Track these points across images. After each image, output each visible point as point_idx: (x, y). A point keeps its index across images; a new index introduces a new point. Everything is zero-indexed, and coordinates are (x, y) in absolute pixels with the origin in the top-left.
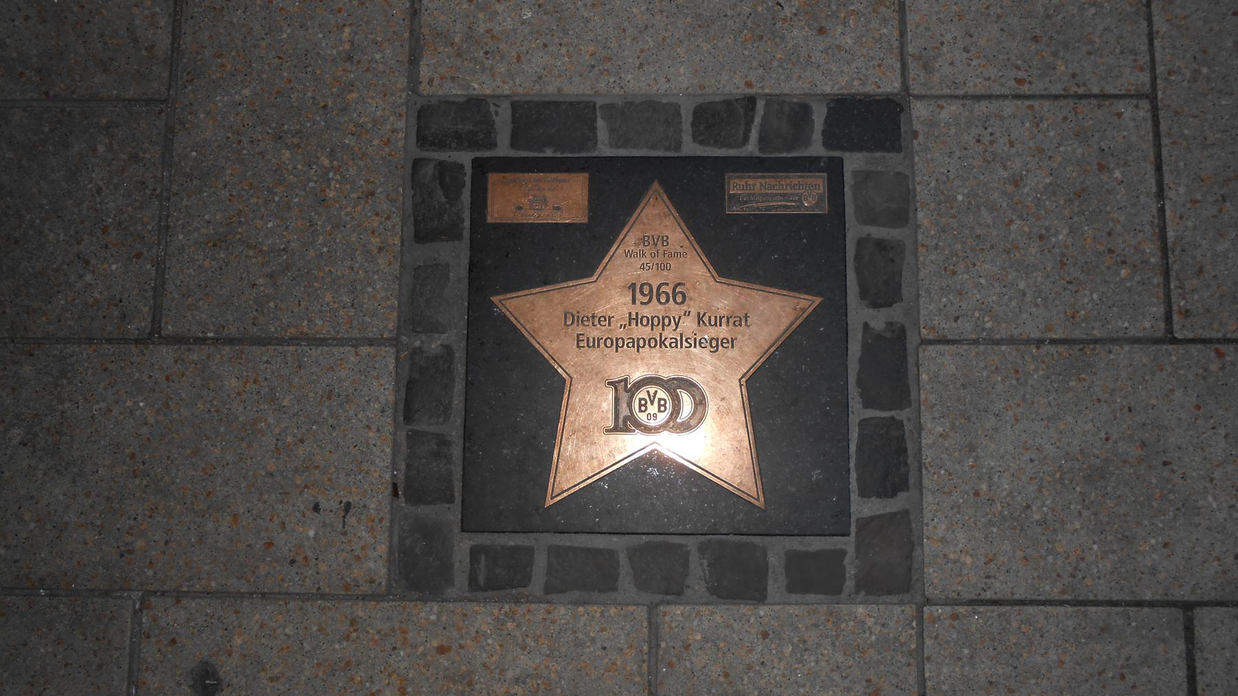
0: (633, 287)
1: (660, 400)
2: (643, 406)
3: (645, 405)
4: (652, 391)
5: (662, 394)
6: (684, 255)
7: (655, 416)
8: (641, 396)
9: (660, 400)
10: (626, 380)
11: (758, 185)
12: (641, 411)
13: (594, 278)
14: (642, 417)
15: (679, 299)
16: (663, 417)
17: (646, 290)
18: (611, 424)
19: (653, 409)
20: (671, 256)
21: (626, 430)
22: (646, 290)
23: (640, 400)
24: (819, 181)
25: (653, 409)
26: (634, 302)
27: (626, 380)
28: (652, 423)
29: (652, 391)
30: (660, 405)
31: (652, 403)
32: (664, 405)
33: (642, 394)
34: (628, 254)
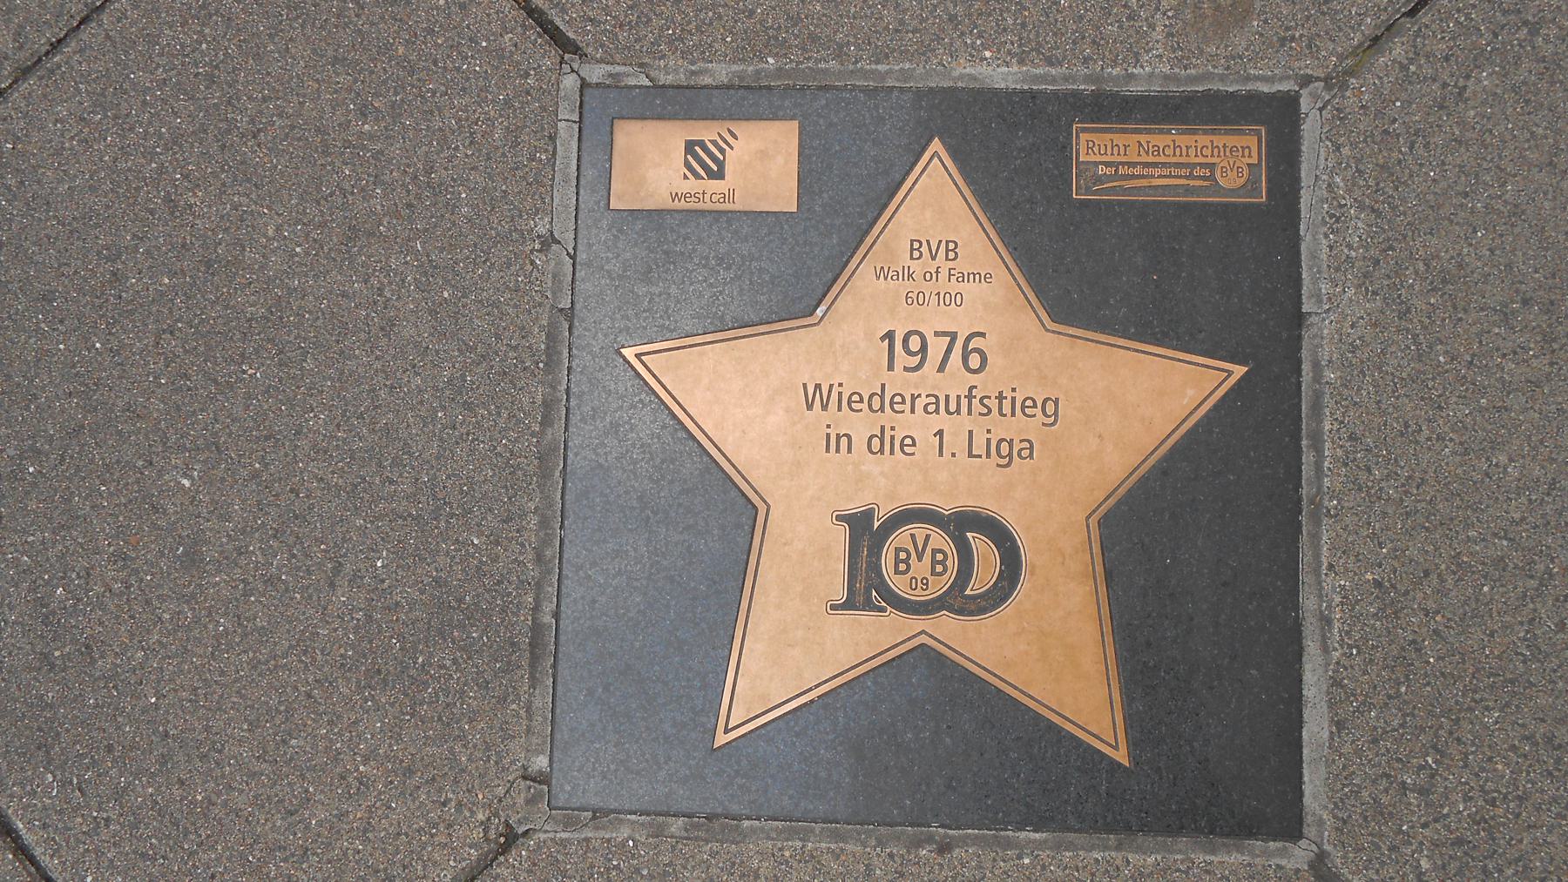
0: (890, 336)
1: (934, 552)
5: (939, 539)
9: (934, 552)
10: (868, 515)
11: (1134, 148)
14: (898, 584)
15: (975, 361)
17: (915, 344)
19: (921, 568)
20: (962, 278)
21: (868, 605)
22: (915, 344)
23: (898, 550)
24: (1252, 142)
25: (921, 568)
26: (891, 367)
30: (934, 562)
32: (943, 563)
33: (900, 537)
34: (881, 273)
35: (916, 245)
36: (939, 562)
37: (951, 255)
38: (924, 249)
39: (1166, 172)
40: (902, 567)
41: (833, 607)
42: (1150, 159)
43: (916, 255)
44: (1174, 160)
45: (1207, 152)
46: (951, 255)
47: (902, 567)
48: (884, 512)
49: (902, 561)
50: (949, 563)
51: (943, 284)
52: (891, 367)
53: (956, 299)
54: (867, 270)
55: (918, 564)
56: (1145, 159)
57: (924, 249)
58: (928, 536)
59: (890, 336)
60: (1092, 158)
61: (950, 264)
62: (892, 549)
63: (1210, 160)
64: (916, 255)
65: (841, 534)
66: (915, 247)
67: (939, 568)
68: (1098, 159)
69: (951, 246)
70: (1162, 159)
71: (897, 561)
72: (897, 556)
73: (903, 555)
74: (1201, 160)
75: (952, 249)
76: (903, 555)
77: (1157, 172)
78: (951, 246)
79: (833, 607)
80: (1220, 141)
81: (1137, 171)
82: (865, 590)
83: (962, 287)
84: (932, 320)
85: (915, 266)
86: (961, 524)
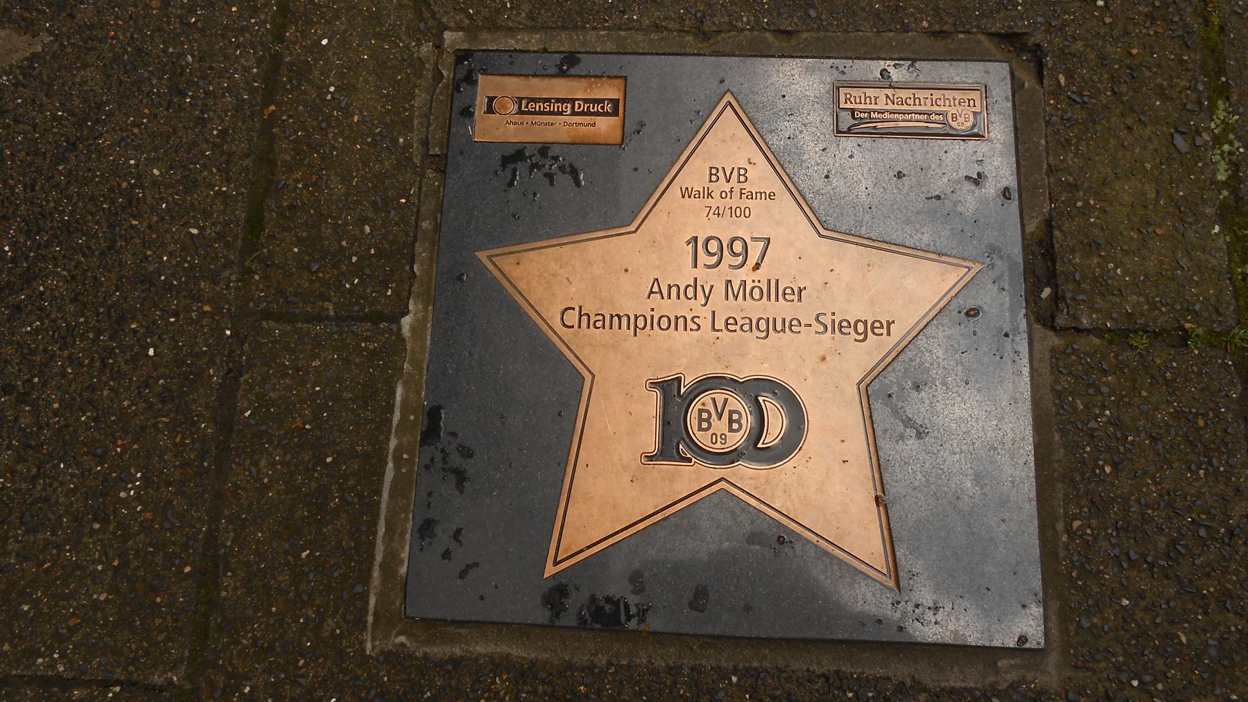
1: (731, 413)
2: (705, 421)
3: (708, 420)
4: (720, 398)
5: (737, 403)
6: (771, 196)
7: (724, 437)
8: (699, 406)
9: (731, 413)
12: (700, 429)
13: (632, 228)
14: (703, 439)
16: (736, 440)
17: (713, 246)
18: (652, 446)
19: (720, 426)
20: (751, 196)
22: (713, 246)
23: (701, 411)
25: (720, 426)
27: (679, 380)
28: (718, 447)
29: (720, 398)
30: (731, 421)
31: (720, 417)
32: (738, 421)
34: (687, 193)
35: (714, 171)
36: (736, 421)
37: (742, 179)
38: (721, 174)
39: (908, 117)
40: (705, 425)
41: (650, 458)
42: (896, 107)
43: (714, 178)
44: (912, 108)
45: (941, 103)
46: (742, 179)
47: (705, 425)
48: (688, 380)
49: (705, 420)
50: (744, 422)
51: (735, 202)
52: (696, 266)
53: (745, 213)
54: (675, 191)
55: (720, 424)
56: (890, 107)
57: (721, 174)
58: (726, 400)
59: (696, 239)
60: (849, 106)
61: (742, 186)
62: (696, 410)
63: (943, 108)
64: (714, 178)
65: (655, 397)
66: (713, 173)
67: (735, 426)
68: (856, 106)
69: (742, 172)
70: (905, 107)
71: (701, 420)
72: (700, 415)
73: (705, 415)
74: (937, 109)
75: (743, 174)
76: (705, 415)
77: (900, 117)
78: (742, 172)
79: (650, 458)
80: (948, 94)
81: (887, 116)
82: (674, 442)
83: (750, 203)
84: (725, 229)
85: (713, 186)
86: (754, 389)
